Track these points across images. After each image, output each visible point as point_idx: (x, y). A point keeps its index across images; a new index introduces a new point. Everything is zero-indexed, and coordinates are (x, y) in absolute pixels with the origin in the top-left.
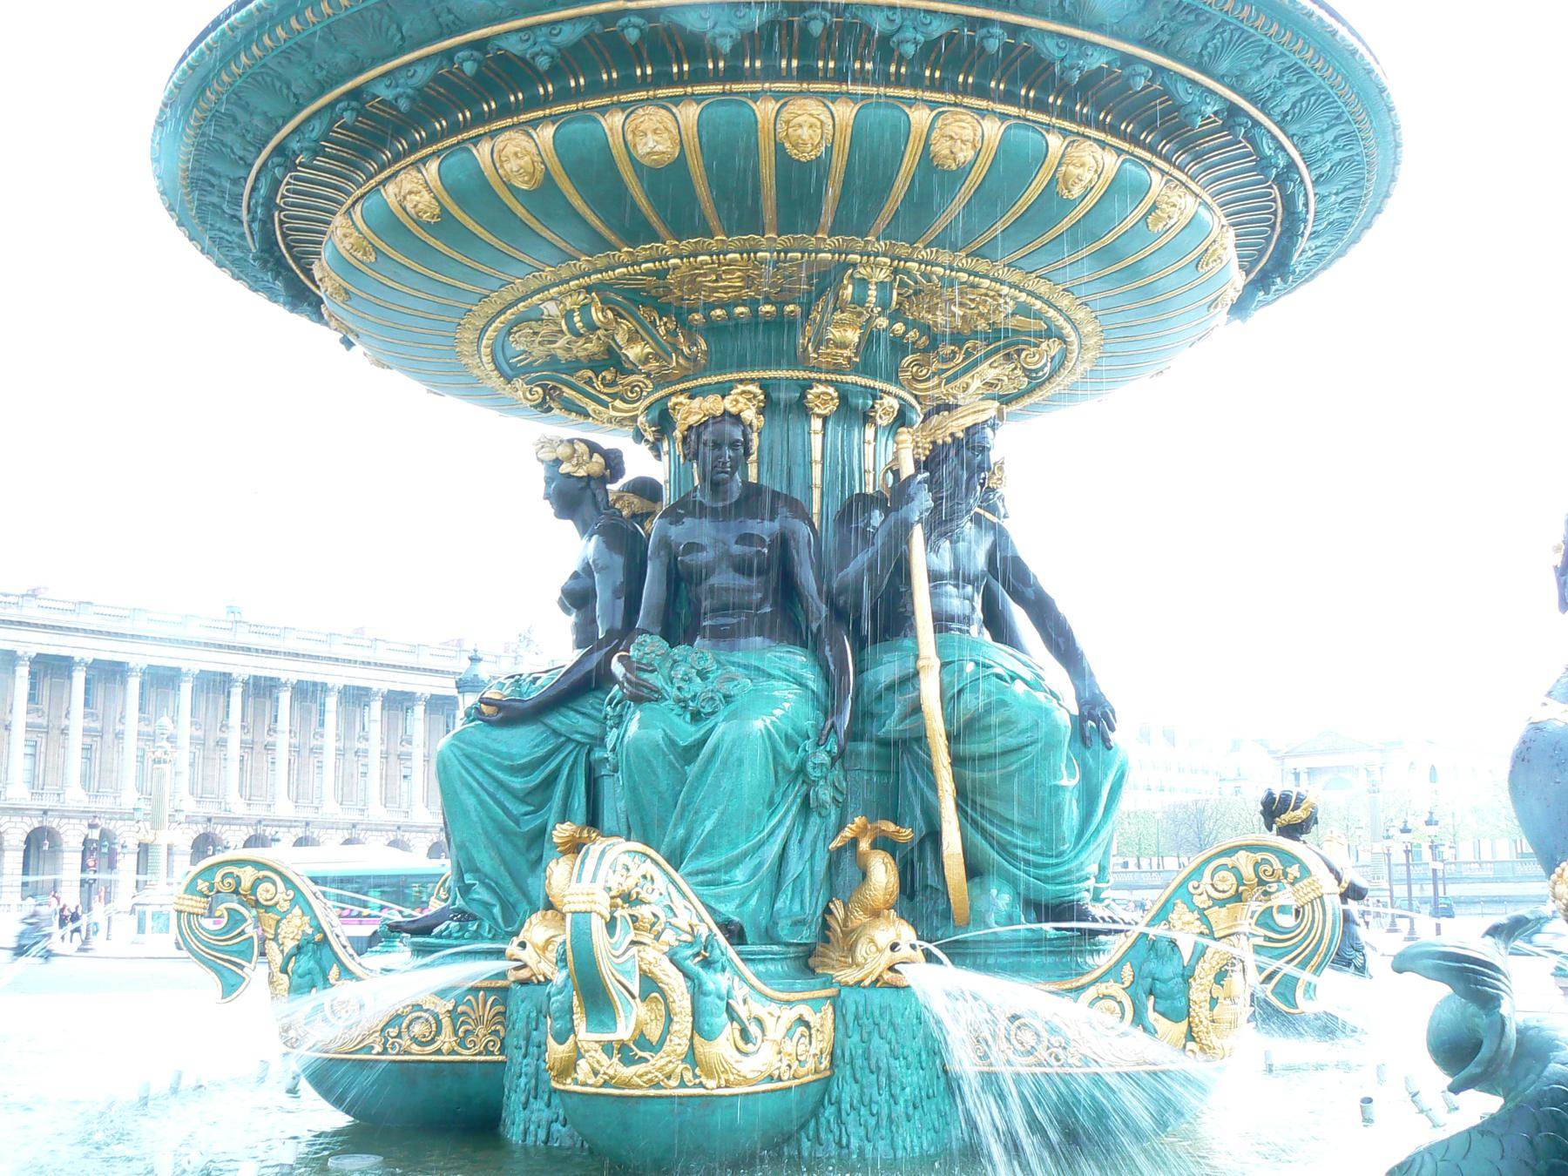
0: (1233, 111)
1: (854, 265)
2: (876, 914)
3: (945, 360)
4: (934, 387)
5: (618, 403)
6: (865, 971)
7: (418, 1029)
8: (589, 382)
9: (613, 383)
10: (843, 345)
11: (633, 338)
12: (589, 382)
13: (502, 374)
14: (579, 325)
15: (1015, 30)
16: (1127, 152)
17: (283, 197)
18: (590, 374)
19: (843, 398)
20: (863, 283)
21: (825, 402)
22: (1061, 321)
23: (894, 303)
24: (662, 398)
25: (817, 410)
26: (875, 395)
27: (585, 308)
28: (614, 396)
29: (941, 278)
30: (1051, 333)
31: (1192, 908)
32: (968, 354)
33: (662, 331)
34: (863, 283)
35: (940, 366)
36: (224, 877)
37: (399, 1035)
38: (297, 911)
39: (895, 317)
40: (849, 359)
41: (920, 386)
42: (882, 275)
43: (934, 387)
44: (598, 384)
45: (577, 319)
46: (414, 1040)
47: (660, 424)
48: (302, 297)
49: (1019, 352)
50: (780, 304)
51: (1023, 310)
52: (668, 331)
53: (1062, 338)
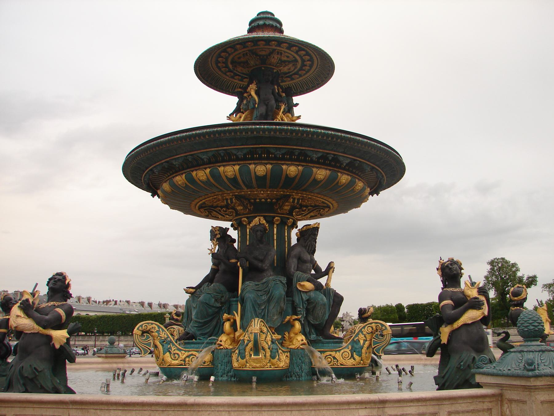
0: (373, 168)
1: (293, 195)
2: (296, 334)
3: (303, 211)
4: (300, 217)
5: (227, 216)
6: (295, 346)
8: (220, 210)
9: (226, 211)
11: (239, 206)
14: (229, 202)
15: (334, 155)
18: (220, 208)
19: (282, 220)
21: (277, 221)
24: (240, 218)
25: (276, 223)
26: (288, 219)
28: (226, 214)
31: (363, 334)
32: (309, 210)
33: (245, 204)
34: (294, 199)
35: (303, 213)
36: (145, 326)
40: (286, 212)
43: (300, 217)
49: (320, 210)
51: (323, 202)
52: (247, 204)
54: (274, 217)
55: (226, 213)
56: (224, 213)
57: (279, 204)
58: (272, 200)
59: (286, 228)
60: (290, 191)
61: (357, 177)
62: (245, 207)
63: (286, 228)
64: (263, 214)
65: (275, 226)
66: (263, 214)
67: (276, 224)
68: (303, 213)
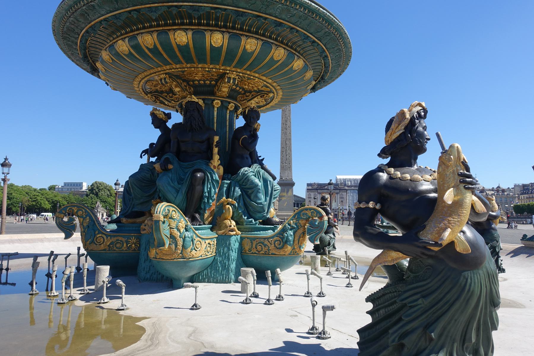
1: (228, 73)
3: (247, 96)
5: (173, 102)
7: (118, 245)
8: (166, 96)
9: (172, 97)
10: (224, 92)
11: (176, 87)
12: (166, 96)
13: (145, 93)
16: (290, 51)
17: (88, 44)
18: (166, 94)
20: (229, 78)
22: (274, 90)
23: (236, 83)
27: (165, 79)
28: (172, 100)
29: (247, 77)
30: (271, 92)
32: (252, 95)
34: (229, 78)
37: (113, 247)
38: (88, 218)
39: (237, 86)
41: (241, 102)
42: (233, 76)
44: (168, 97)
45: (163, 81)
46: (117, 248)
47: (181, 107)
48: (94, 71)
49: (264, 95)
50: (211, 82)
52: (185, 86)
53: (273, 93)
54: (214, 100)
55: (172, 99)
56: (170, 99)
57: (218, 86)
58: (211, 82)
59: (228, 112)
60: (222, 68)
61: (297, 54)
62: (183, 90)
63: (228, 112)
64: (202, 97)
65: (216, 109)
66: (202, 97)
67: (216, 107)
68: (247, 98)
